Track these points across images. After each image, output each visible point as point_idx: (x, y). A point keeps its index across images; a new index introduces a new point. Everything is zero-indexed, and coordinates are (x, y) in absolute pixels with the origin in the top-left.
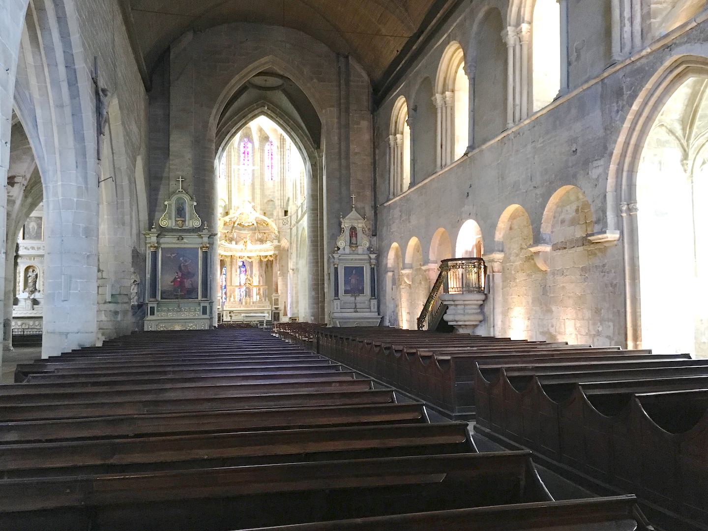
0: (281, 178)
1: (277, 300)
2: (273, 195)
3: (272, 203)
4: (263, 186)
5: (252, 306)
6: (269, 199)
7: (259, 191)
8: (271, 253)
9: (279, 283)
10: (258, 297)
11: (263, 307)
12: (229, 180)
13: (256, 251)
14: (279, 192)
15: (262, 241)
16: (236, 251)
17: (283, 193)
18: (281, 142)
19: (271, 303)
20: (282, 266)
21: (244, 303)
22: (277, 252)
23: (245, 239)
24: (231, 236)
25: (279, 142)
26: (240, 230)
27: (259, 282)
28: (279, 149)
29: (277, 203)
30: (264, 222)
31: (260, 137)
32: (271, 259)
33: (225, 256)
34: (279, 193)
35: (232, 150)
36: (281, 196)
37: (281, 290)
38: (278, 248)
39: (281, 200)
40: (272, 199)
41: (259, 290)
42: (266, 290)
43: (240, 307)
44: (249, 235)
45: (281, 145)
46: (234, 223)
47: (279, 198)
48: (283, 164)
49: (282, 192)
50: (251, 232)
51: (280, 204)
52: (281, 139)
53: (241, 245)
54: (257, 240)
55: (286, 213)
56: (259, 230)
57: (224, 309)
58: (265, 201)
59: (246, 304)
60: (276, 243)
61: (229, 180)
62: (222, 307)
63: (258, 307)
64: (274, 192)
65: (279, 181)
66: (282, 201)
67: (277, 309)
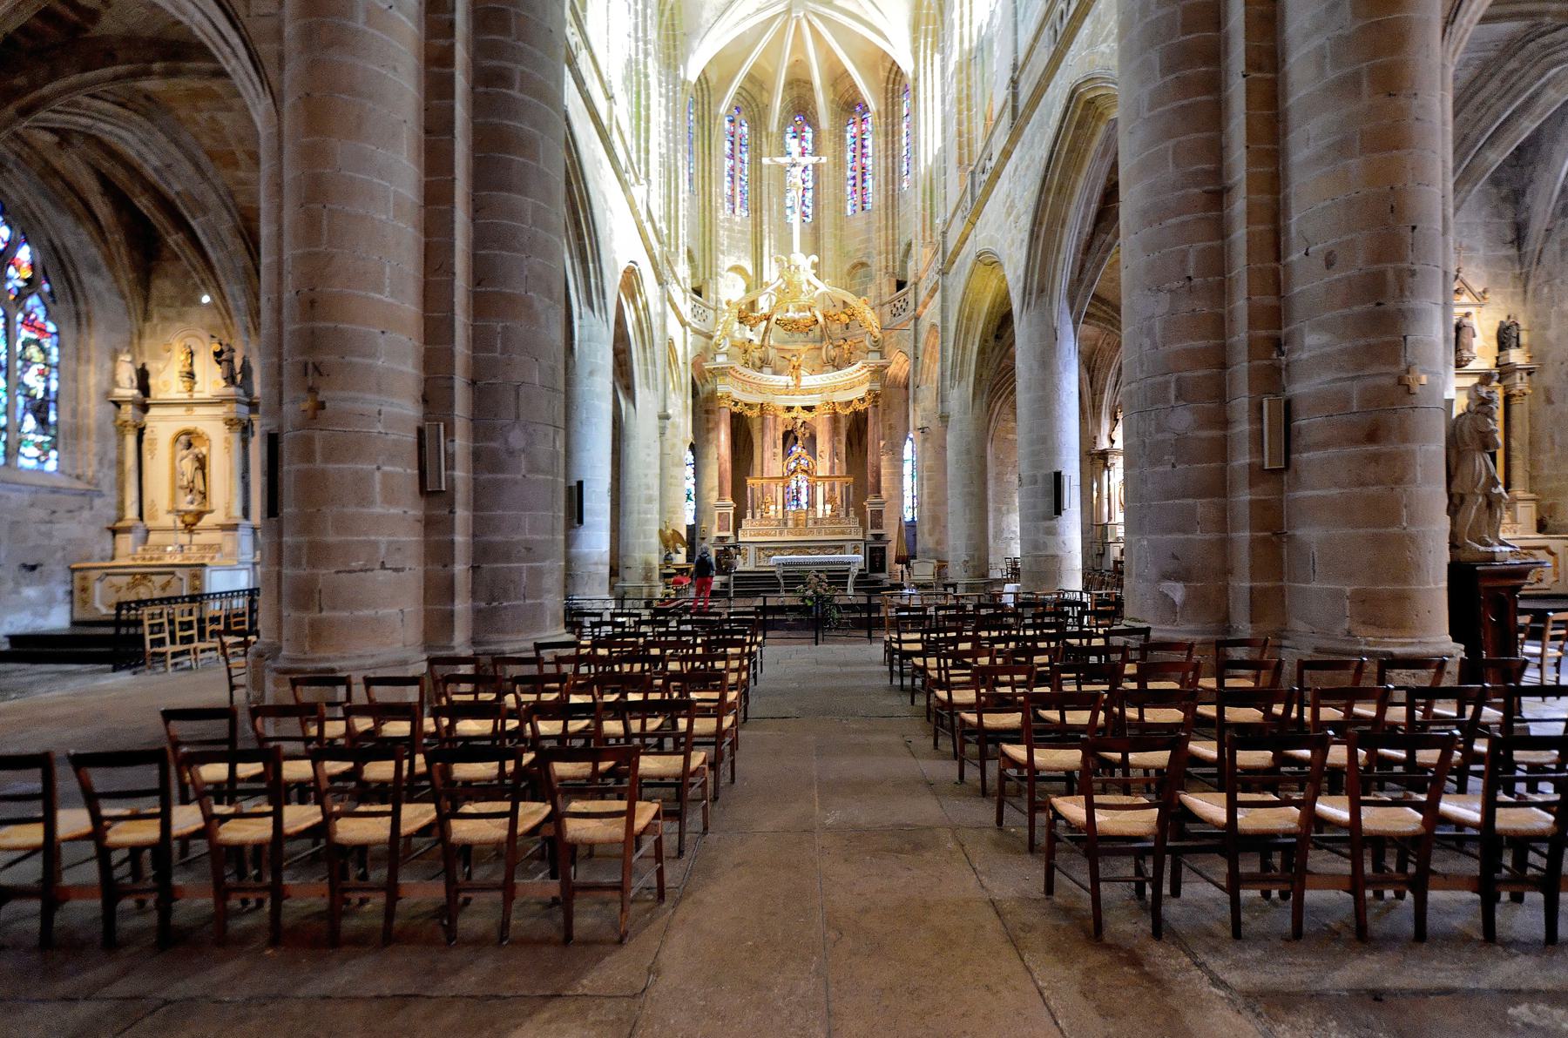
0: (887, 197)
1: (878, 515)
3: (861, 271)
5: (811, 532)
8: (861, 392)
9: (883, 471)
10: (828, 507)
11: (843, 533)
13: (821, 390)
14: (883, 233)
15: (836, 364)
17: (893, 235)
18: (886, 99)
19: (863, 523)
20: (891, 427)
21: (790, 523)
22: (877, 387)
25: (883, 101)
27: (832, 468)
28: (883, 120)
29: (877, 262)
31: (833, 101)
32: (861, 407)
34: (883, 239)
35: (764, 140)
36: (887, 245)
37: (887, 490)
38: (879, 372)
39: (887, 253)
40: (864, 260)
41: (832, 489)
42: (848, 488)
45: (886, 105)
47: (883, 248)
48: (893, 157)
49: (890, 232)
50: (810, 345)
51: (884, 263)
52: (887, 93)
53: (783, 380)
54: (825, 364)
55: (901, 285)
56: (830, 338)
59: (797, 525)
60: (874, 359)
62: (736, 533)
64: (869, 240)
65: (883, 202)
66: (890, 256)
67: (878, 537)
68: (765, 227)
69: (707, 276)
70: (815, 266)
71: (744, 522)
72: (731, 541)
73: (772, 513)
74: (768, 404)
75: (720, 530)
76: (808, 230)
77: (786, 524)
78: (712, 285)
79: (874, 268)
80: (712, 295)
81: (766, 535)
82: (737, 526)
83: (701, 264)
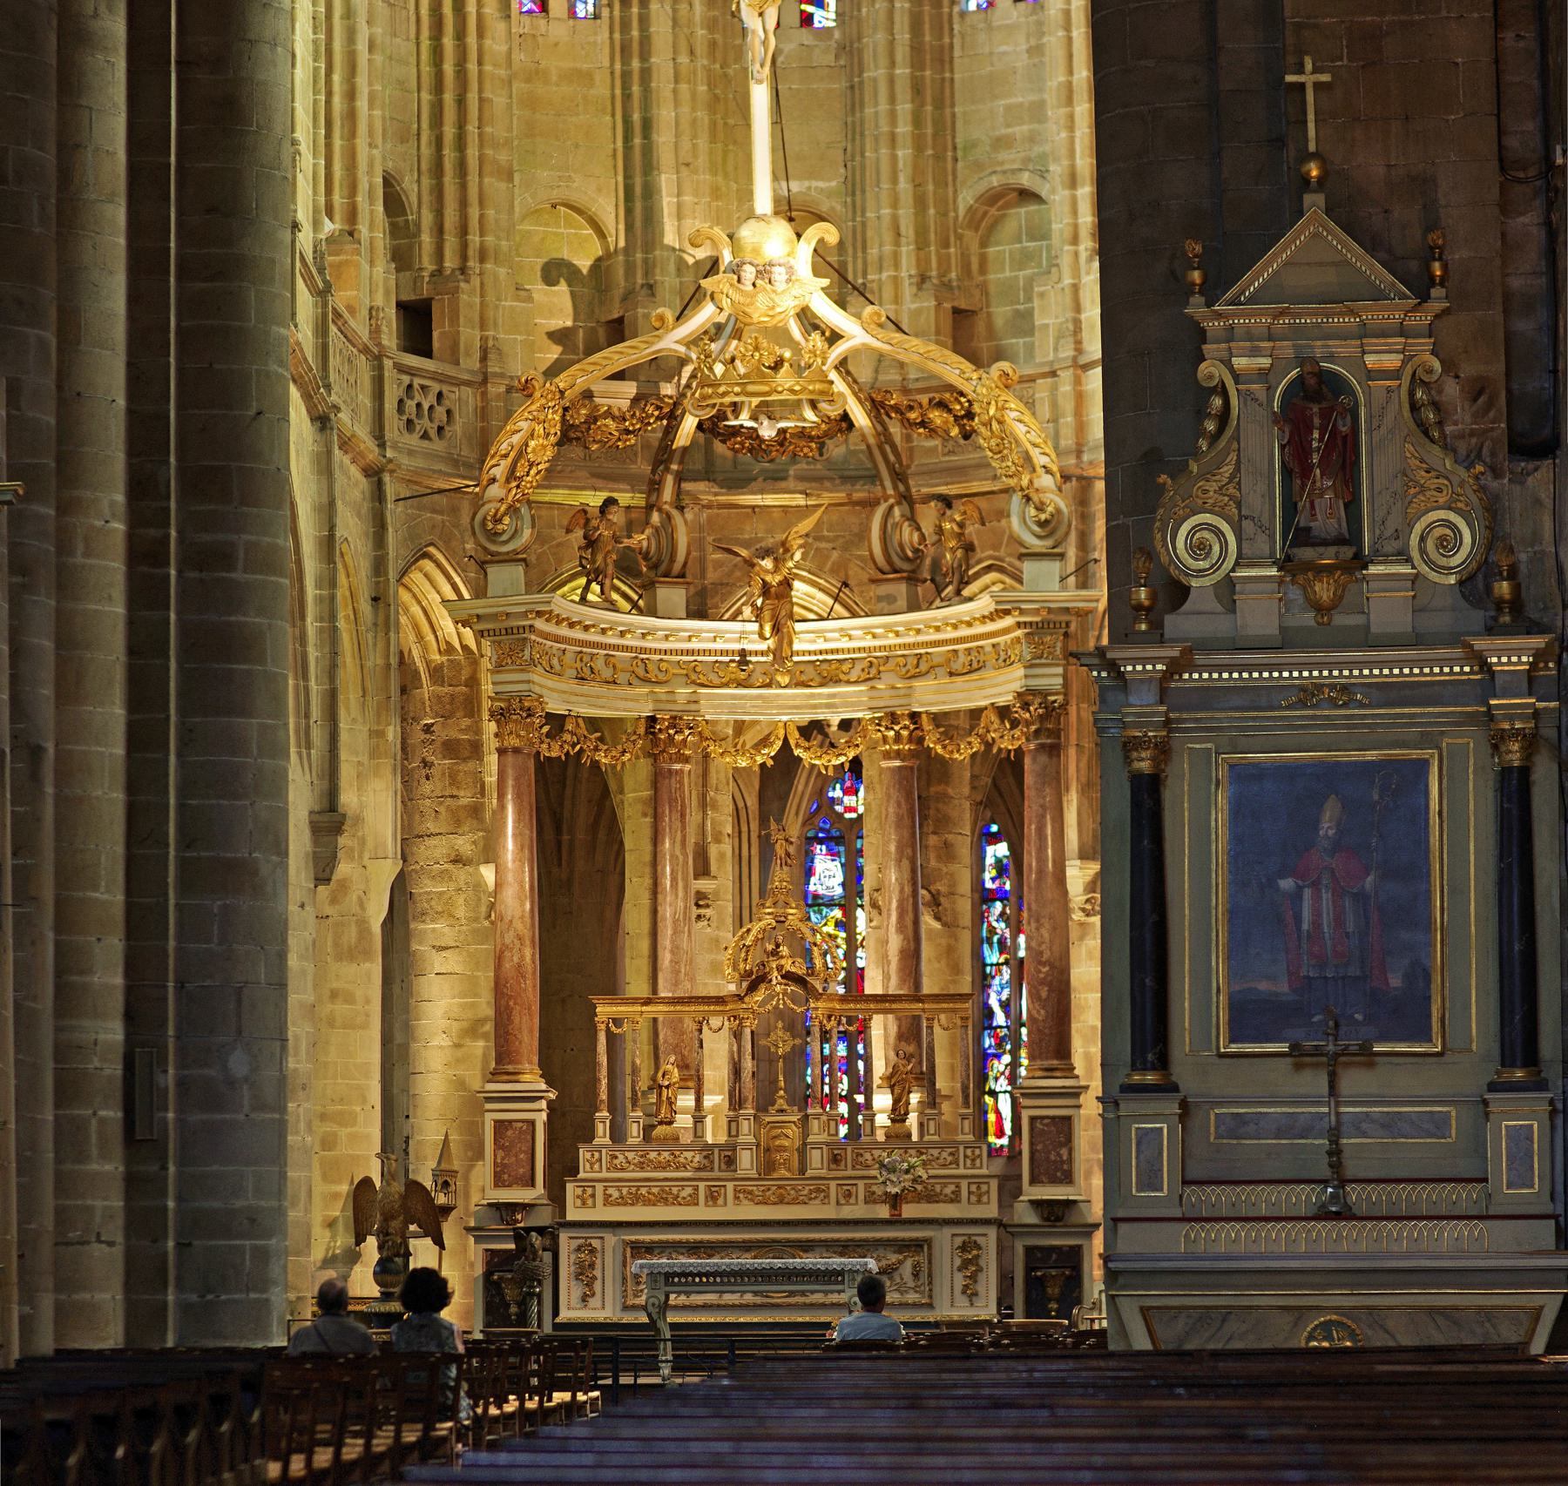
2: (1032, 139)
3: (1023, 211)
4: (943, 58)
6: (995, 181)
7: (905, 108)
8: (1003, 686)
12: (625, 26)
13: (872, 667)
16: (696, 673)
21: (746, 1160)
23: (767, 563)
24: (641, 539)
26: (739, 482)
27: (911, 958)
30: (945, 396)
32: (1008, 742)
33: (593, 723)
40: (1025, 180)
43: (713, 1198)
44: (806, 525)
46: (673, 418)
57: (572, 1214)
58: (966, 198)
61: (625, 26)
62: (557, 1197)
64: (1037, 111)
68: (660, 60)
69: (450, 263)
70: (823, 261)
71: (584, 1154)
72: (543, 1218)
73: (684, 1121)
74: (674, 722)
75: (499, 1182)
76: (824, 57)
77: (730, 1162)
78: (468, 296)
79: (1059, 226)
80: (469, 335)
81: (664, 1199)
82: (562, 1168)
83: (427, 218)
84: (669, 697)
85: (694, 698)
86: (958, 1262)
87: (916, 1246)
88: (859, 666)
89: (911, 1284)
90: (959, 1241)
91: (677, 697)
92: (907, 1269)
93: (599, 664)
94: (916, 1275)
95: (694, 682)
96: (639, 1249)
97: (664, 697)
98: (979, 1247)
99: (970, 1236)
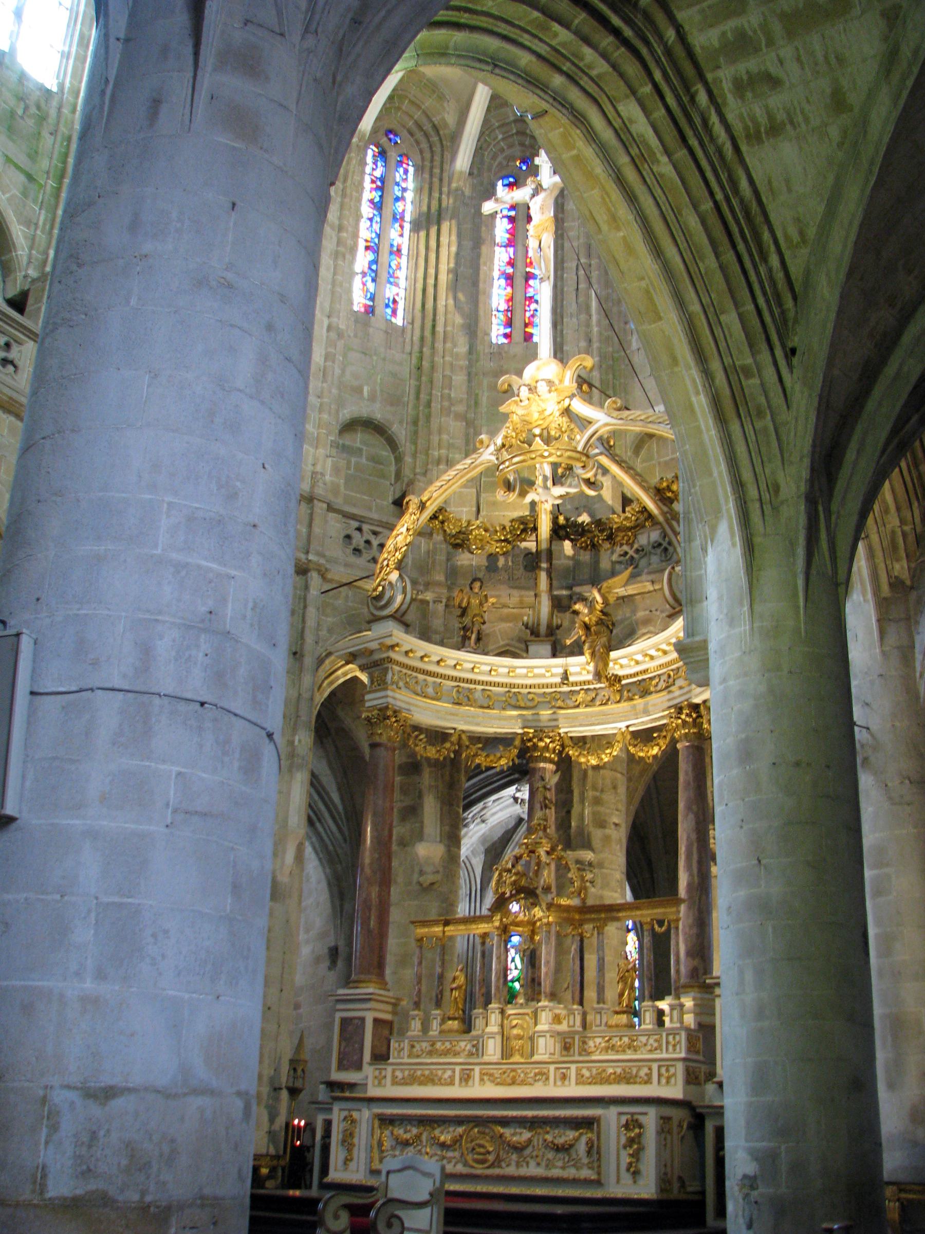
63: (580, 1080)
84: (536, 717)
85: (554, 717)
86: (623, 1140)
87: (588, 1123)
88: (663, 678)
89: (585, 1160)
90: (623, 1119)
91: (542, 718)
92: (582, 1147)
93: (478, 695)
94: (589, 1152)
95: (553, 707)
96: (386, 1121)
97: (530, 718)
98: (640, 1126)
99: (632, 1114)
